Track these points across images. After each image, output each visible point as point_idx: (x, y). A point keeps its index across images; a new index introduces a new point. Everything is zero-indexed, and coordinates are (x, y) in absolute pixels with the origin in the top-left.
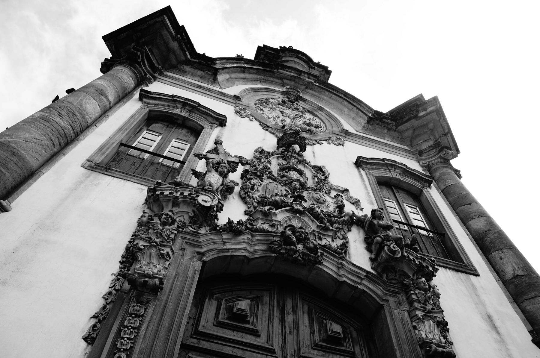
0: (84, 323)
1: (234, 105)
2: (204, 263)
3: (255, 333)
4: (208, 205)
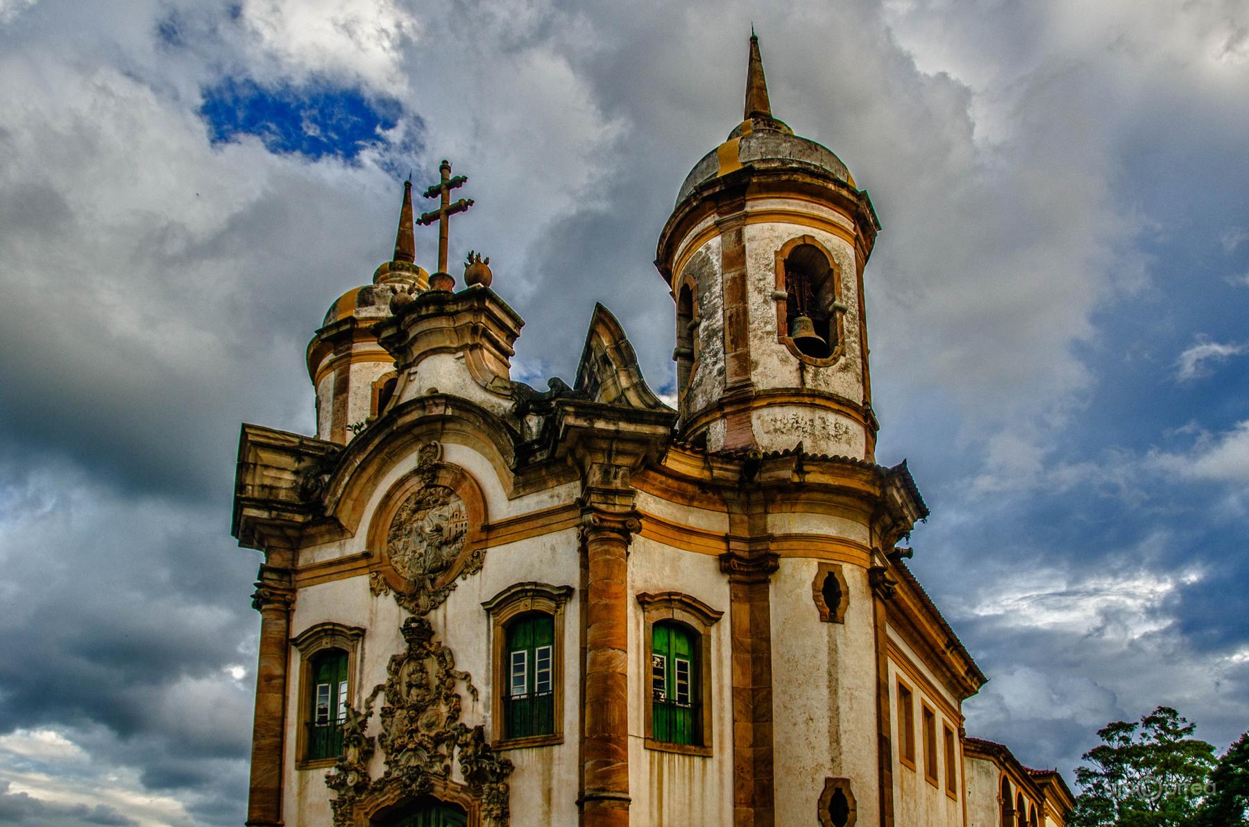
1: (367, 570)
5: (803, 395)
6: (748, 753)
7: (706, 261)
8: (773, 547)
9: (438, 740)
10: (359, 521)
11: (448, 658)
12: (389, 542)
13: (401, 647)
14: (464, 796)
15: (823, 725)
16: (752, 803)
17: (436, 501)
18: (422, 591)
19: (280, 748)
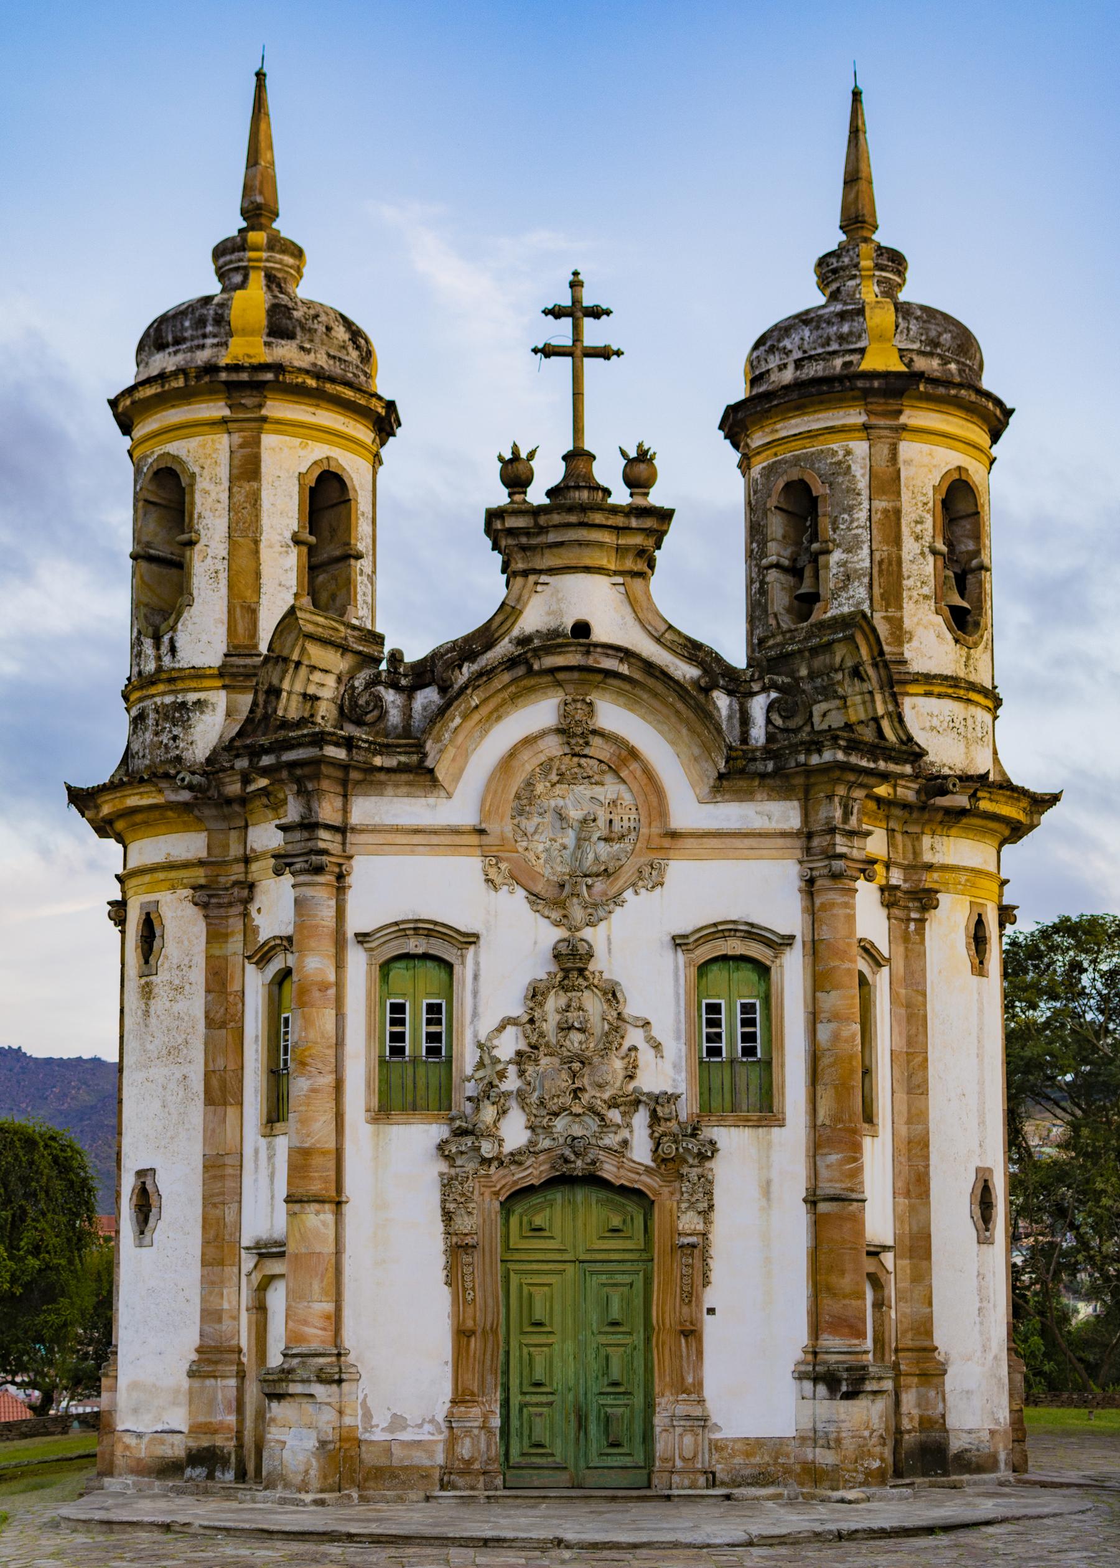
0: (441, 1275)
1: (478, 851)
2: (501, 1203)
3: (552, 1238)
4: (490, 1156)
5: (960, 688)
6: (903, 1130)
7: (843, 468)
10: (457, 777)
11: (618, 995)
12: (513, 818)
13: (541, 968)
14: (648, 1180)
16: (908, 1194)
17: (589, 777)
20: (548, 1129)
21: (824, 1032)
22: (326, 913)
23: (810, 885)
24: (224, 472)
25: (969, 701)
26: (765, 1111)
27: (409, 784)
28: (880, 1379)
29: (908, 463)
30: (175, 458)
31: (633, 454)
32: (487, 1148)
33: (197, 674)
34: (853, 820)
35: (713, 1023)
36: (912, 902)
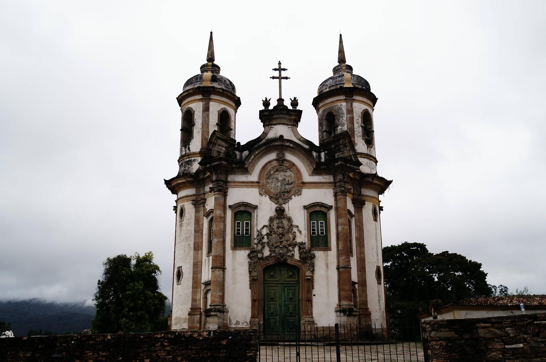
0: (248, 286)
8: (363, 198)
9: (290, 245)
13: (273, 214)
15: (375, 250)
16: (360, 271)
18: (280, 197)
19: (224, 242)
20: (274, 251)
21: (340, 228)
22: (222, 200)
23: (336, 195)
24: (201, 110)
25: (371, 159)
26: (326, 247)
27: (242, 172)
28: (356, 312)
29: (355, 107)
30: (191, 108)
31: (293, 99)
32: (260, 255)
33: (194, 154)
34: (346, 179)
35: (314, 227)
36: (359, 204)
